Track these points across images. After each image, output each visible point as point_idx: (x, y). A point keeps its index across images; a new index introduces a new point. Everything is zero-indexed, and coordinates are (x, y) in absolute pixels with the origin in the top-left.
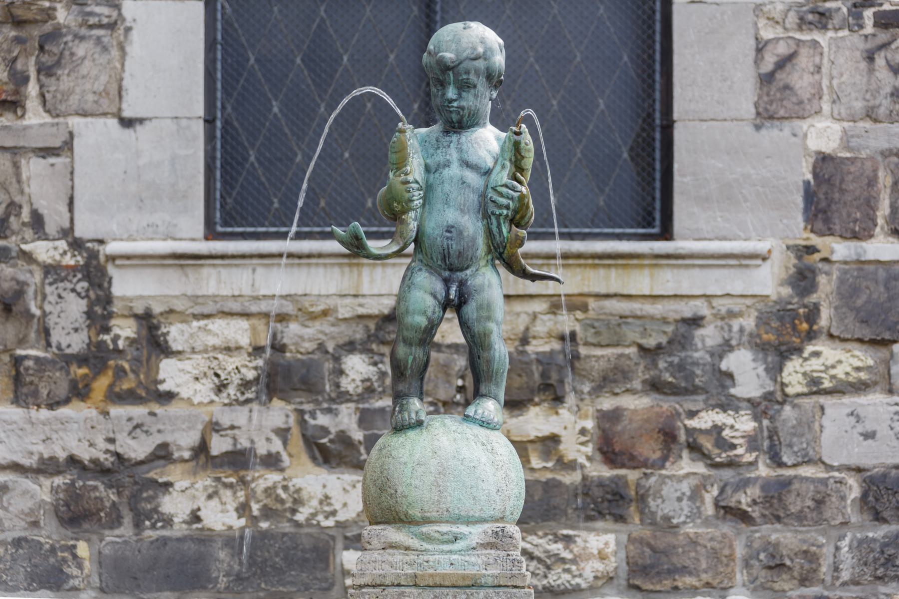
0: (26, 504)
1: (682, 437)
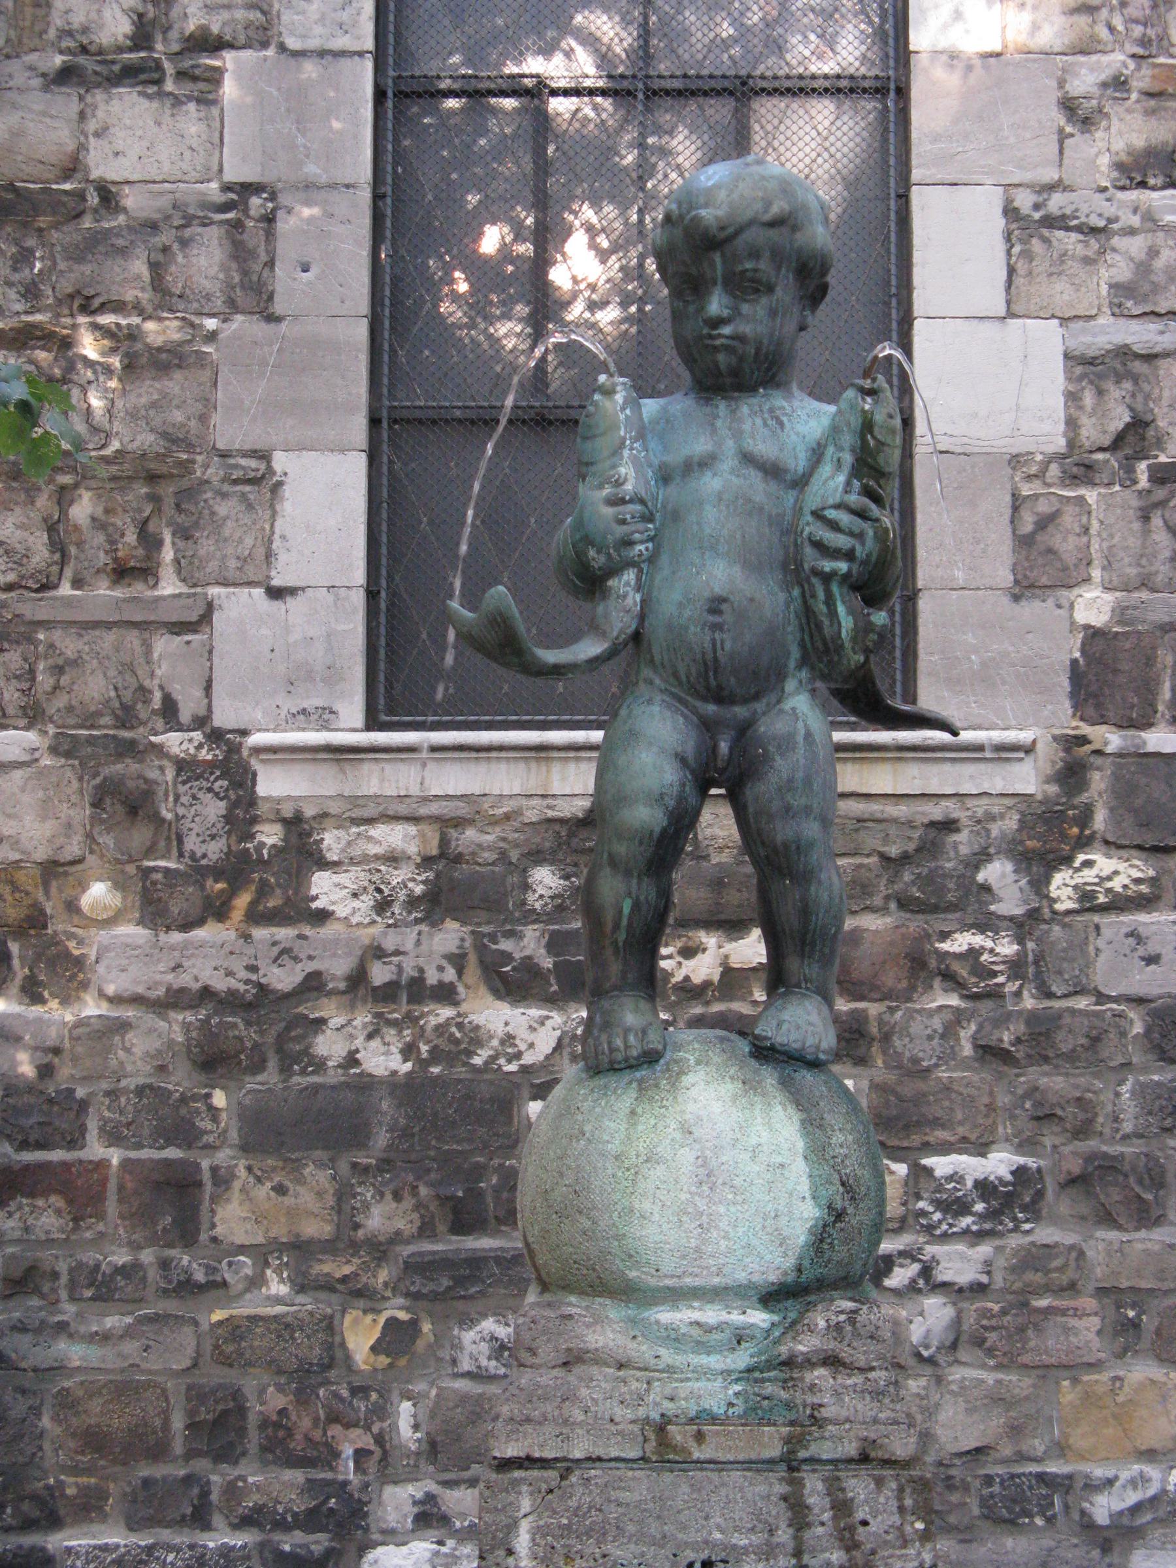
0: (156, 1044)
1: (933, 963)
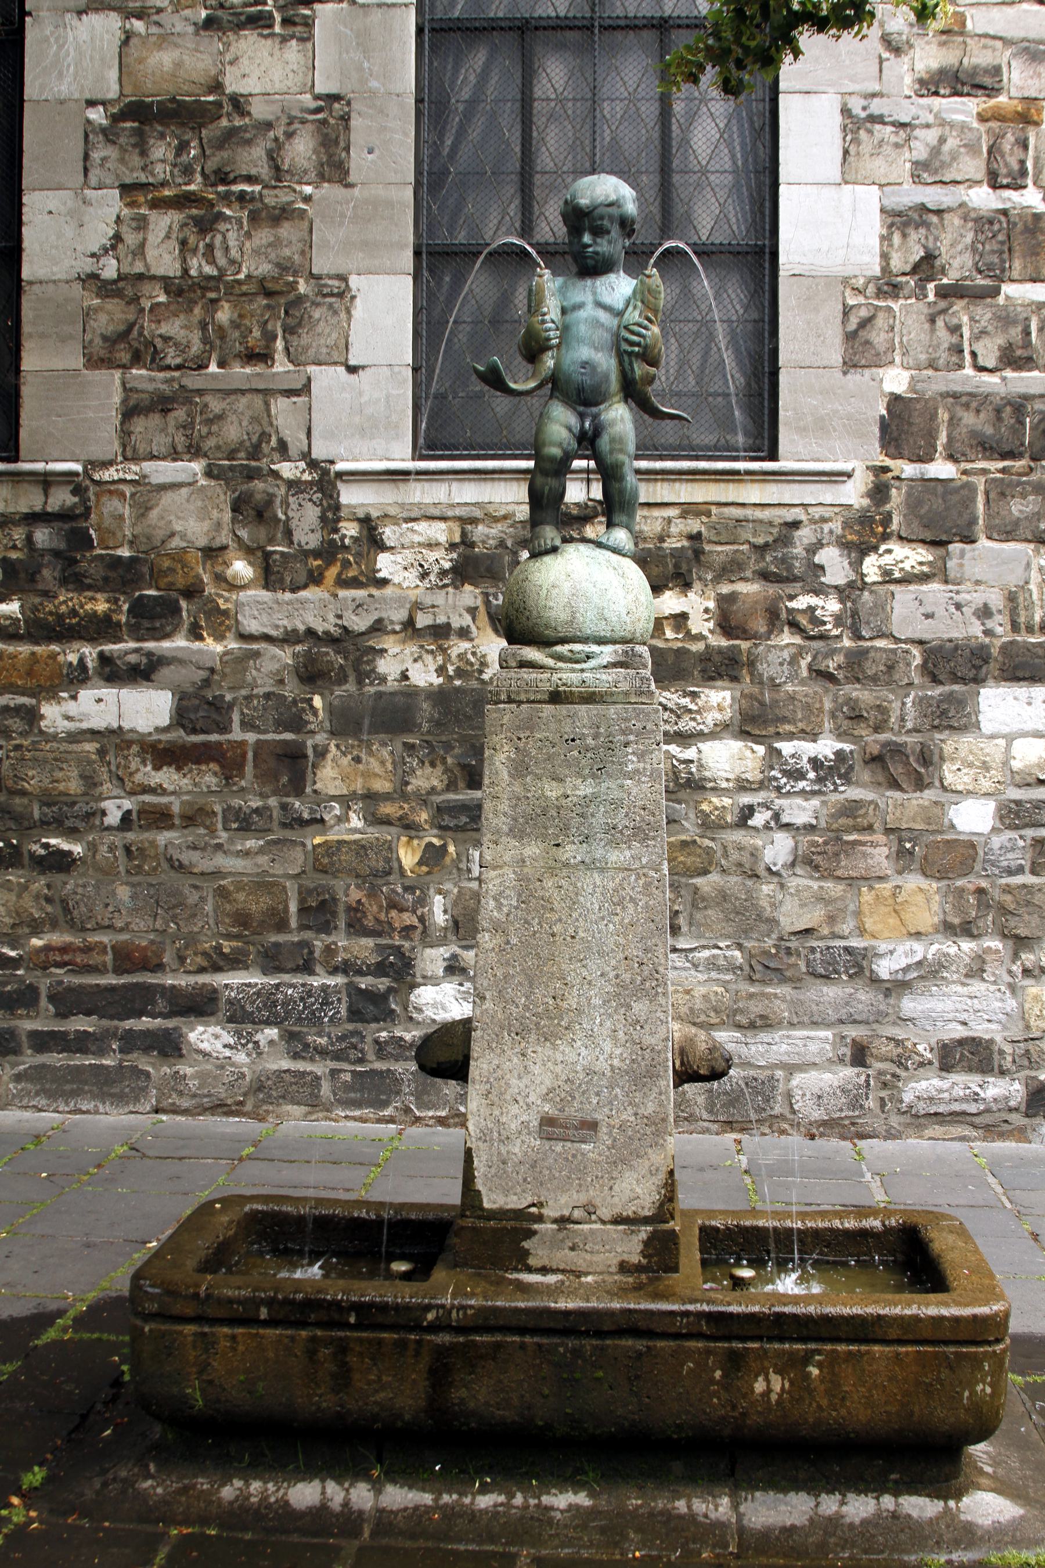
0: (275, 666)
1: (784, 615)
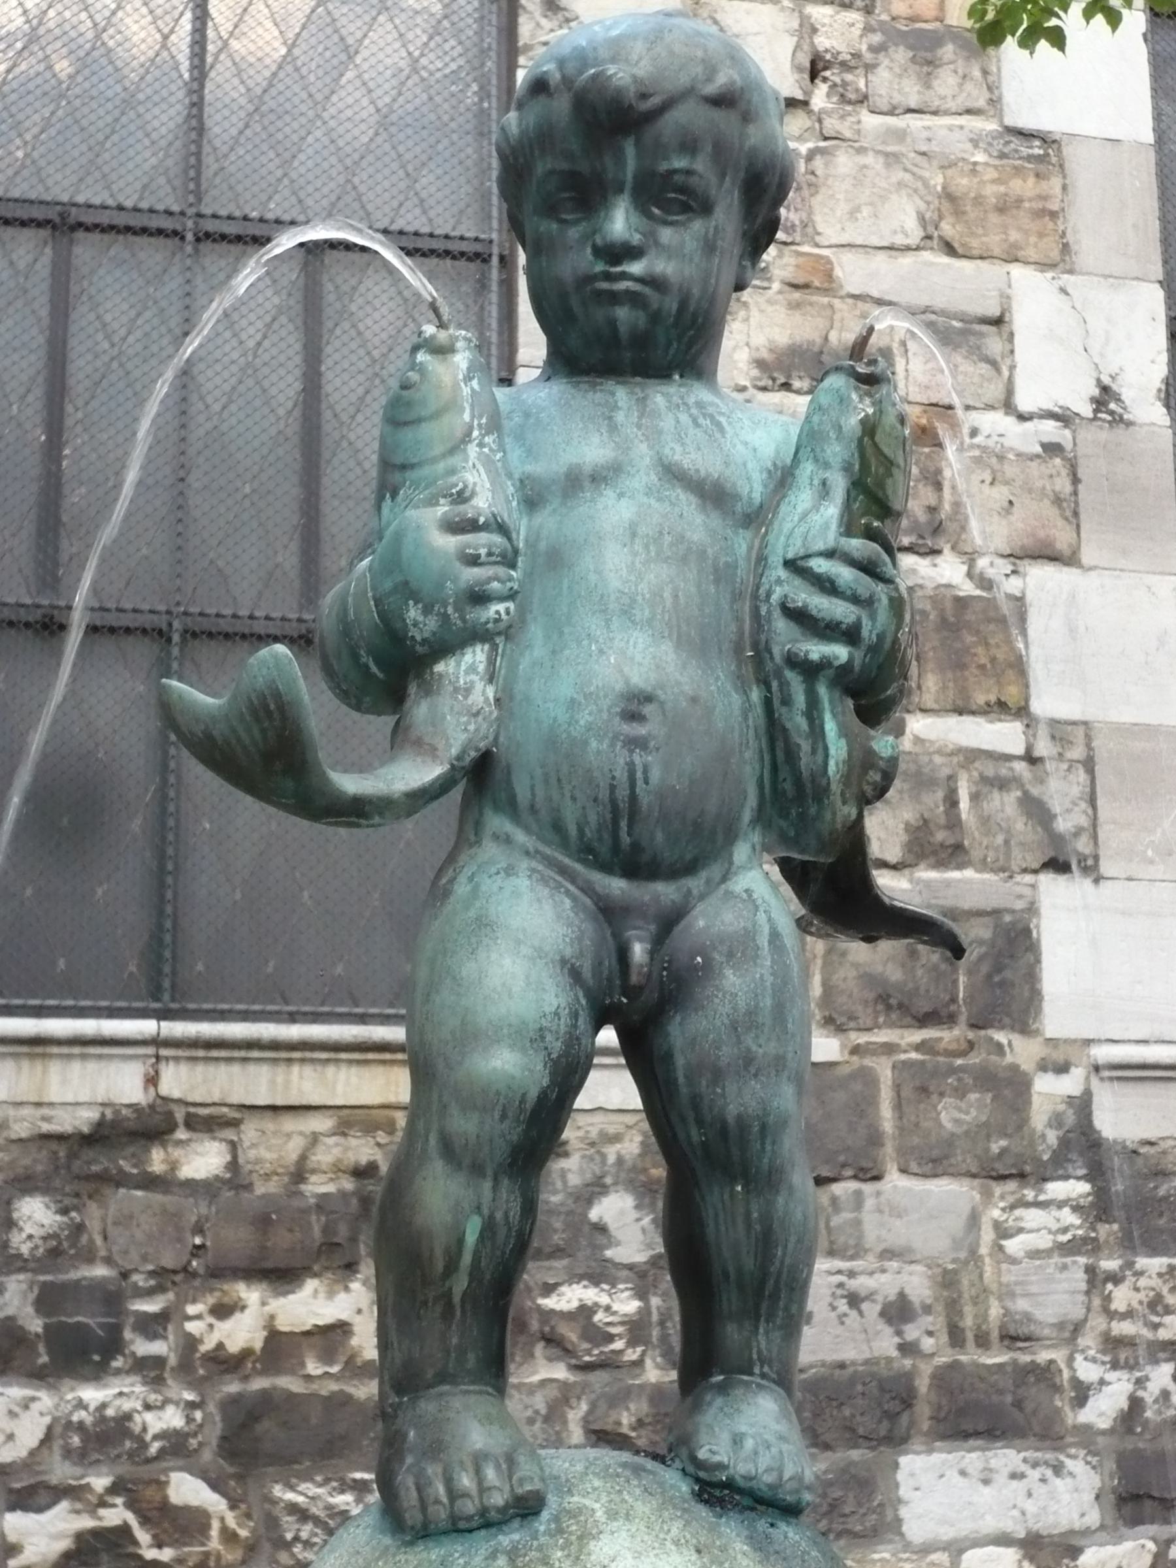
1: (534, 1325)
